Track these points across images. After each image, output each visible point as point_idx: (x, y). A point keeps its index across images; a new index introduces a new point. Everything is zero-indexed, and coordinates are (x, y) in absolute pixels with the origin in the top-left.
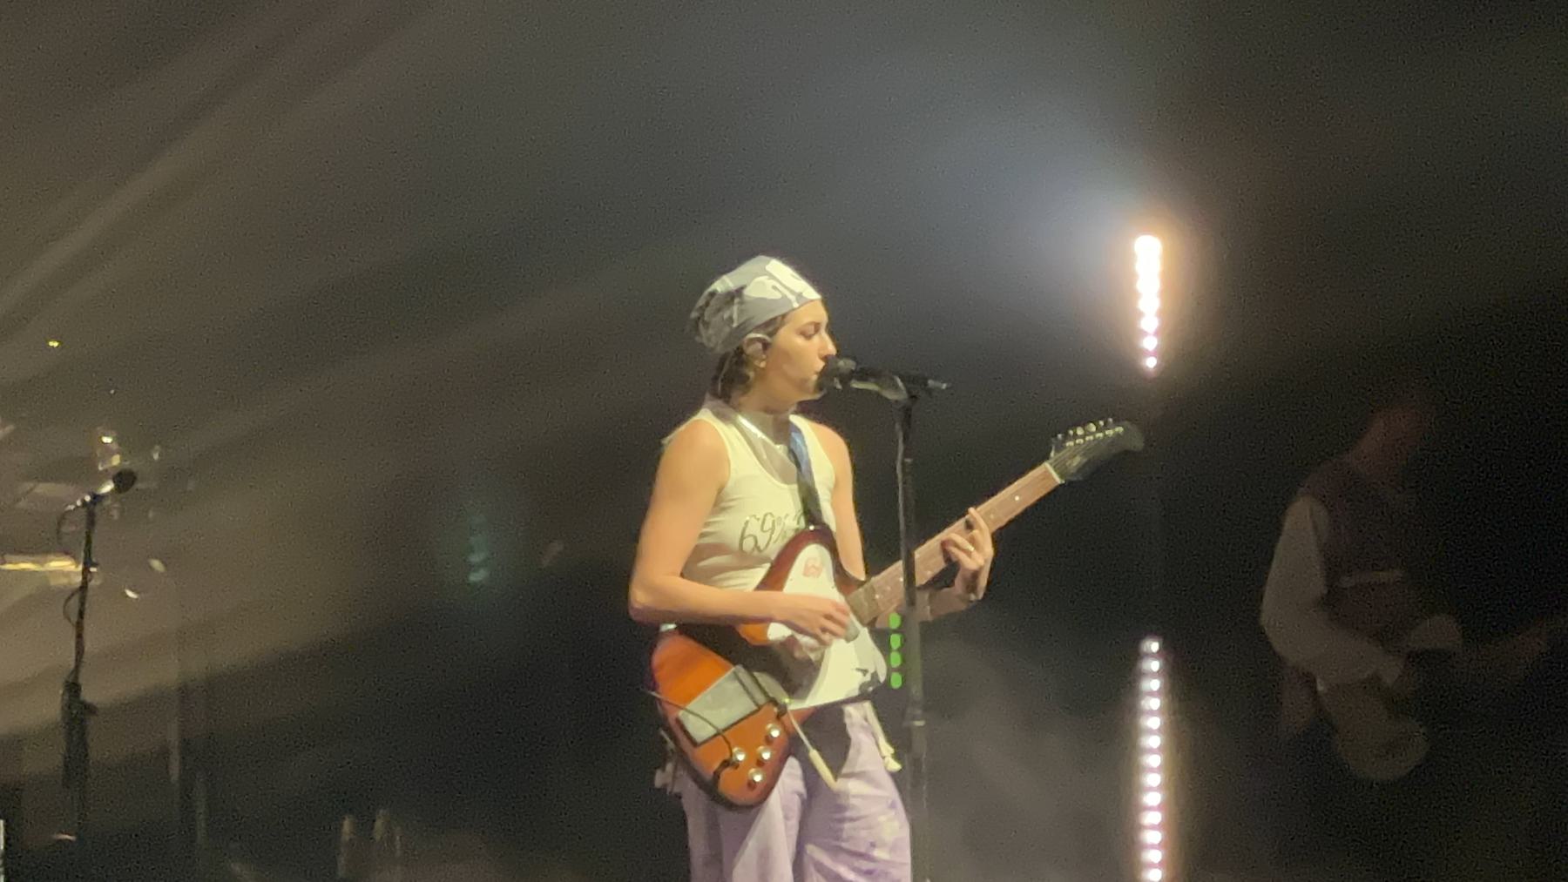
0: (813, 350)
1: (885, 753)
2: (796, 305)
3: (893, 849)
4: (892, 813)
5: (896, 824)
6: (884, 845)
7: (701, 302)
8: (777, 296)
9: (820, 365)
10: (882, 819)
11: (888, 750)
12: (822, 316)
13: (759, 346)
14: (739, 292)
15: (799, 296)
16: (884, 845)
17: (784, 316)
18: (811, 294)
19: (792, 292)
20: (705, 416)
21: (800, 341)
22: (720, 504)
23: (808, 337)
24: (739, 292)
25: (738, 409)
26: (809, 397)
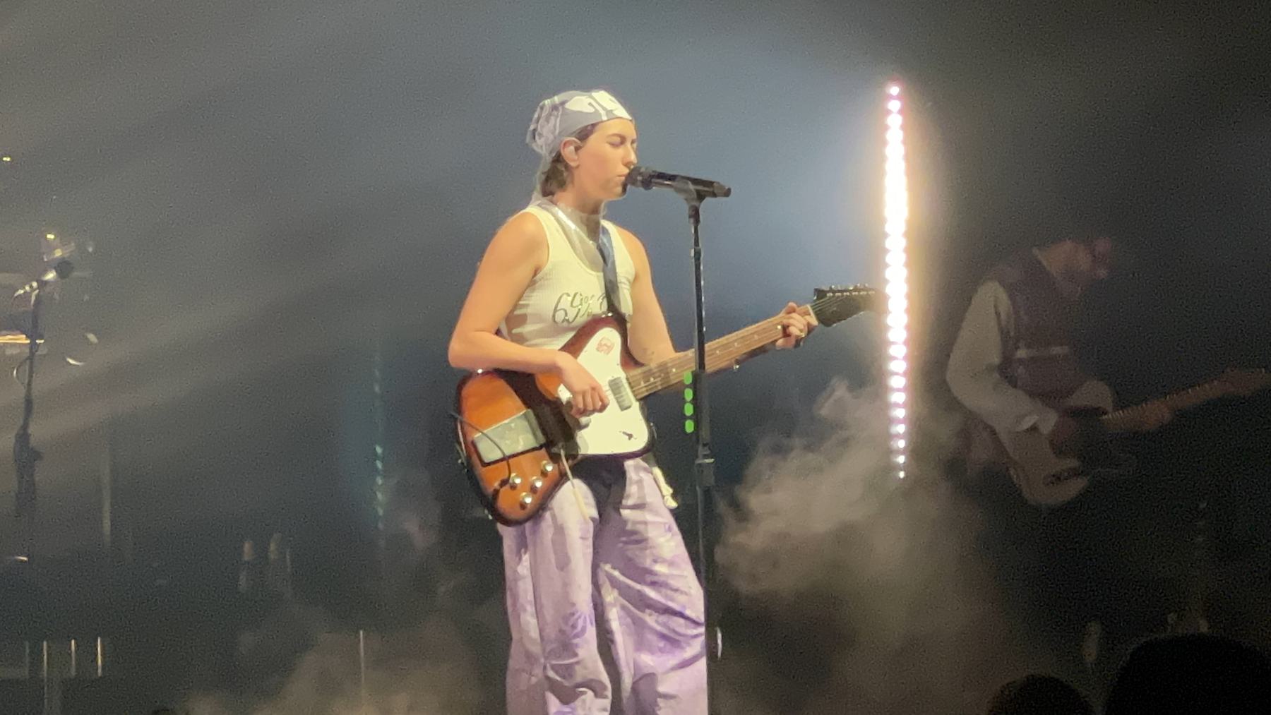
0: (620, 160)
1: (665, 492)
2: (605, 118)
3: (671, 564)
4: (669, 535)
5: (672, 544)
6: (664, 561)
7: (536, 116)
8: (591, 110)
9: (626, 171)
10: (662, 540)
11: (667, 490)
12: (631, 132)
13: (572, 148)
14: (563, 103)
15: (609, 112)
16: (664, 561)
17: (594, 125)
18: (621, 112)
19: (604, 109)
20: (532, 209)
21: (608, 147)
22: (532, 282)
23: (614, 145)
24: (563, 103)
25: (554, 203)
26: (615, 199)
